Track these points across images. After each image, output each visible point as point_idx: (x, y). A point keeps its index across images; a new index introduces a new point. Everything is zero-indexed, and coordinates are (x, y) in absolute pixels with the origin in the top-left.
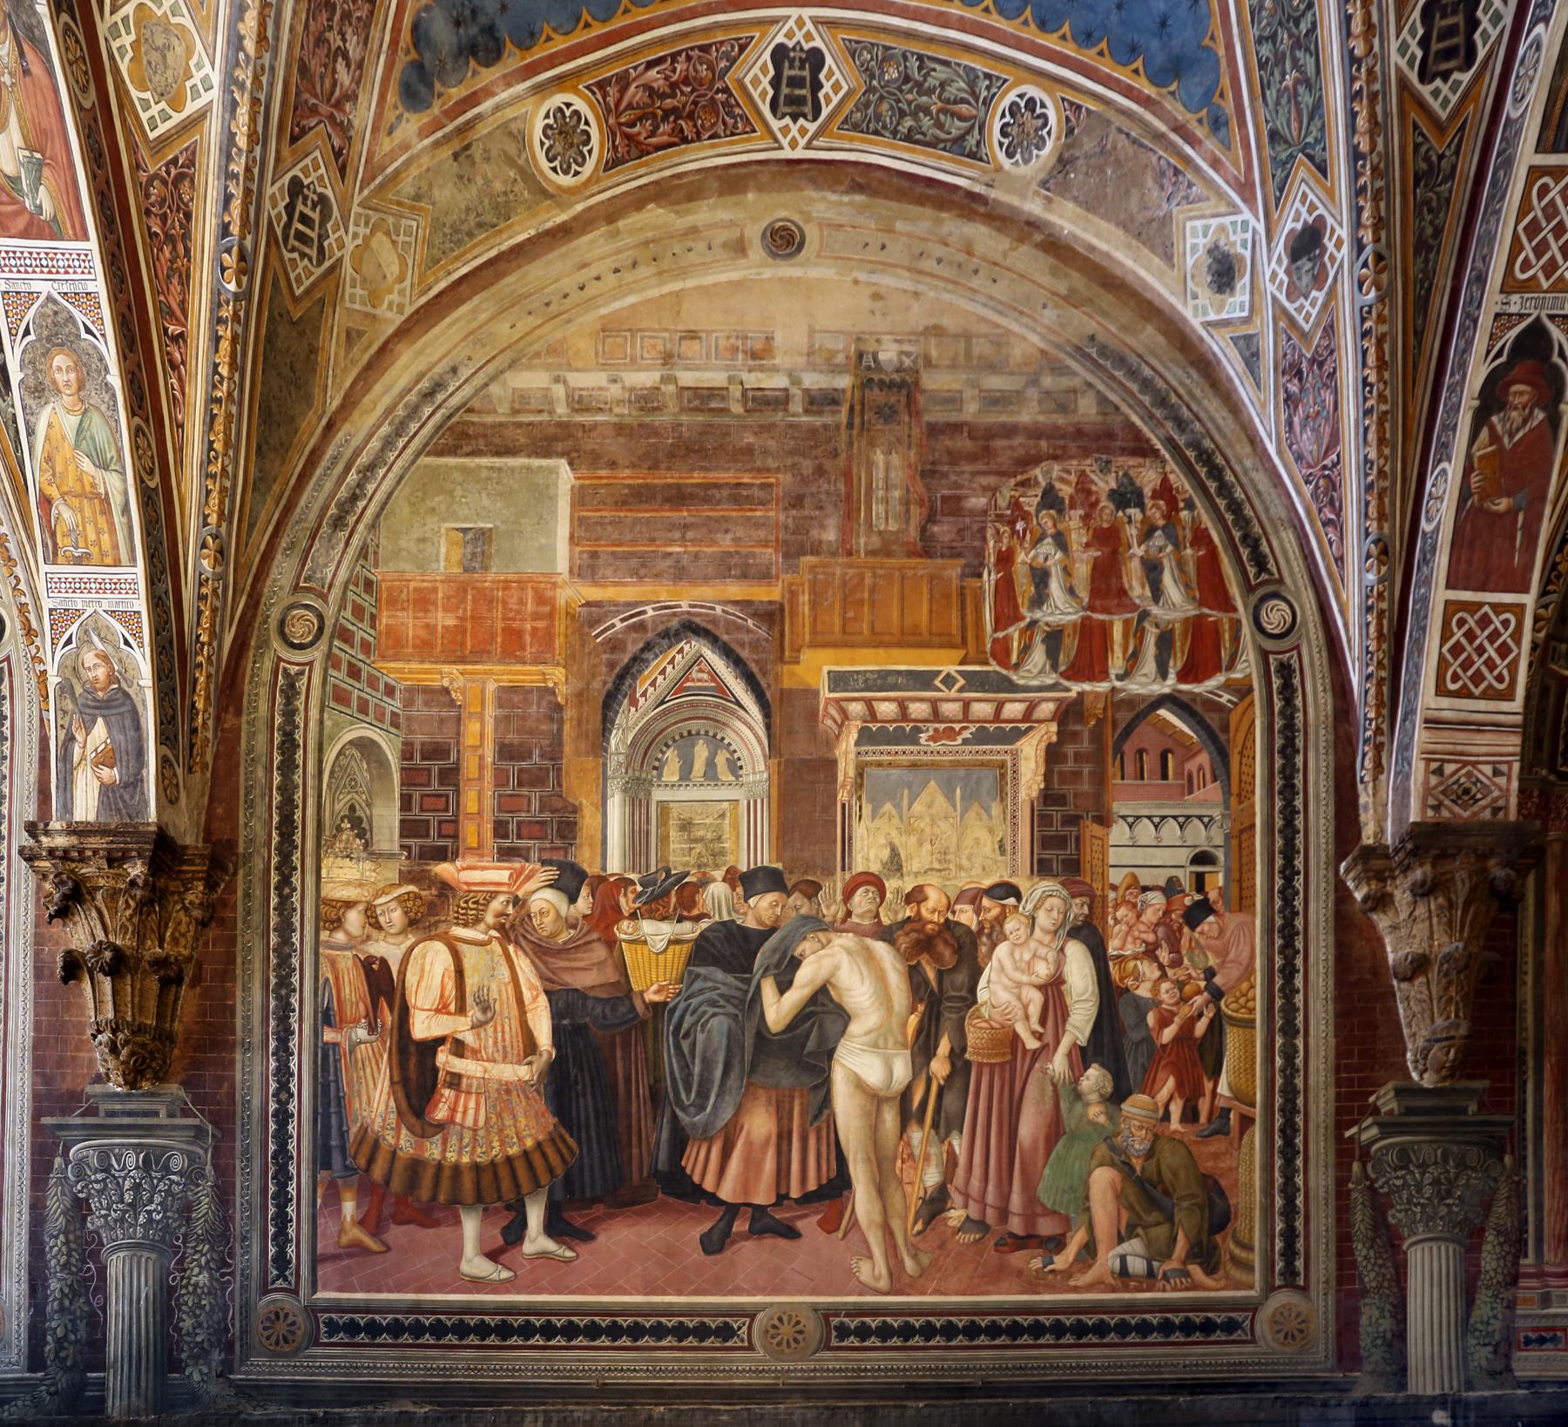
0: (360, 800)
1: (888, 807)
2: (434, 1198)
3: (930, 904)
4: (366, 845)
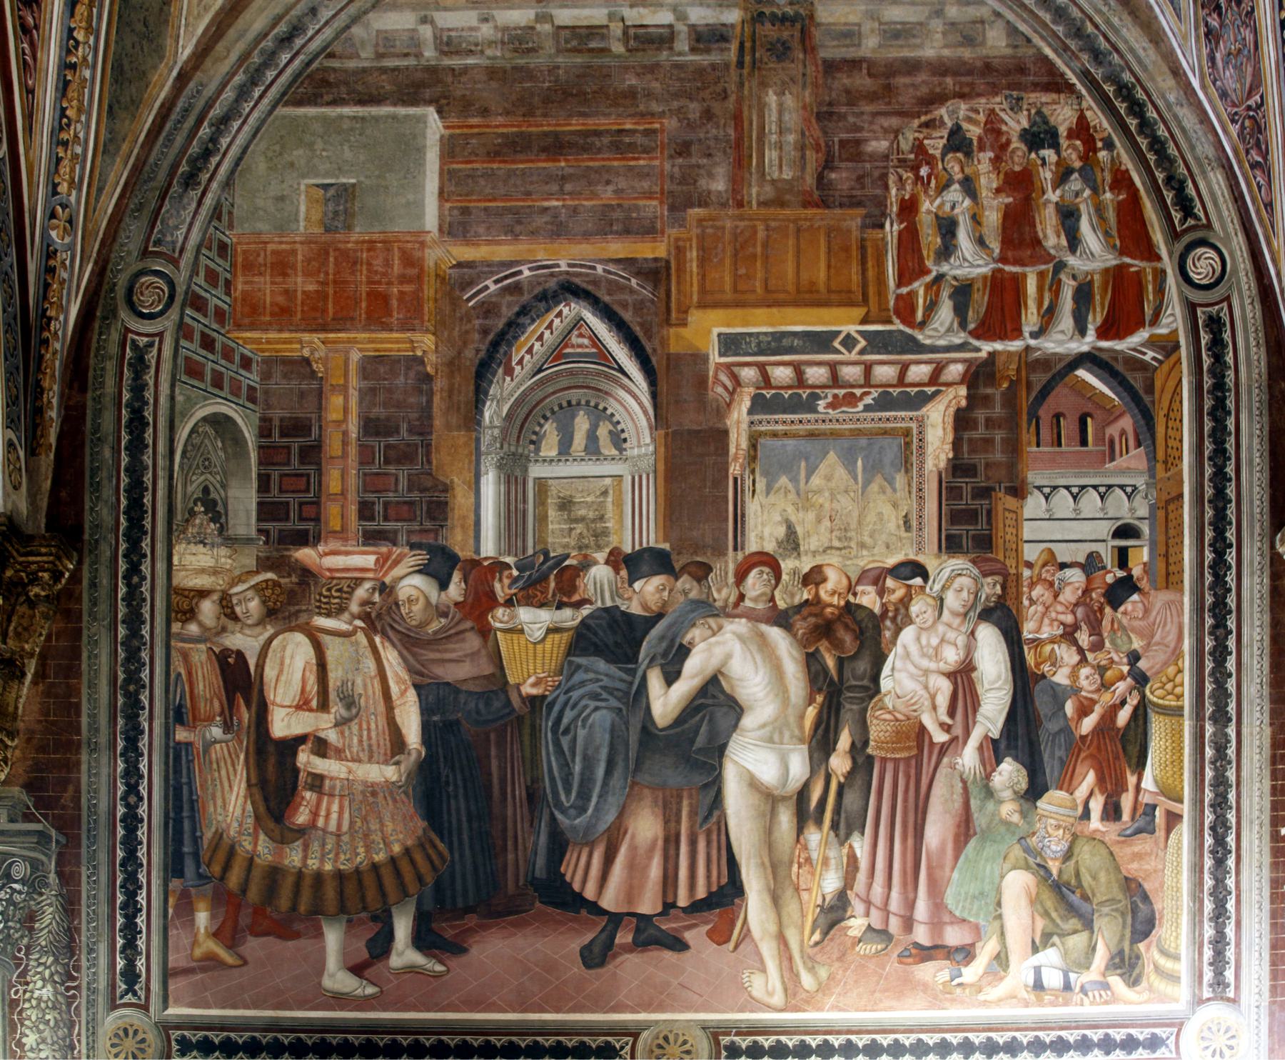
0: (214, 480)
1: (783, 480)
2: (294, 908)
3: (830, 585)
4: (222, 529)
